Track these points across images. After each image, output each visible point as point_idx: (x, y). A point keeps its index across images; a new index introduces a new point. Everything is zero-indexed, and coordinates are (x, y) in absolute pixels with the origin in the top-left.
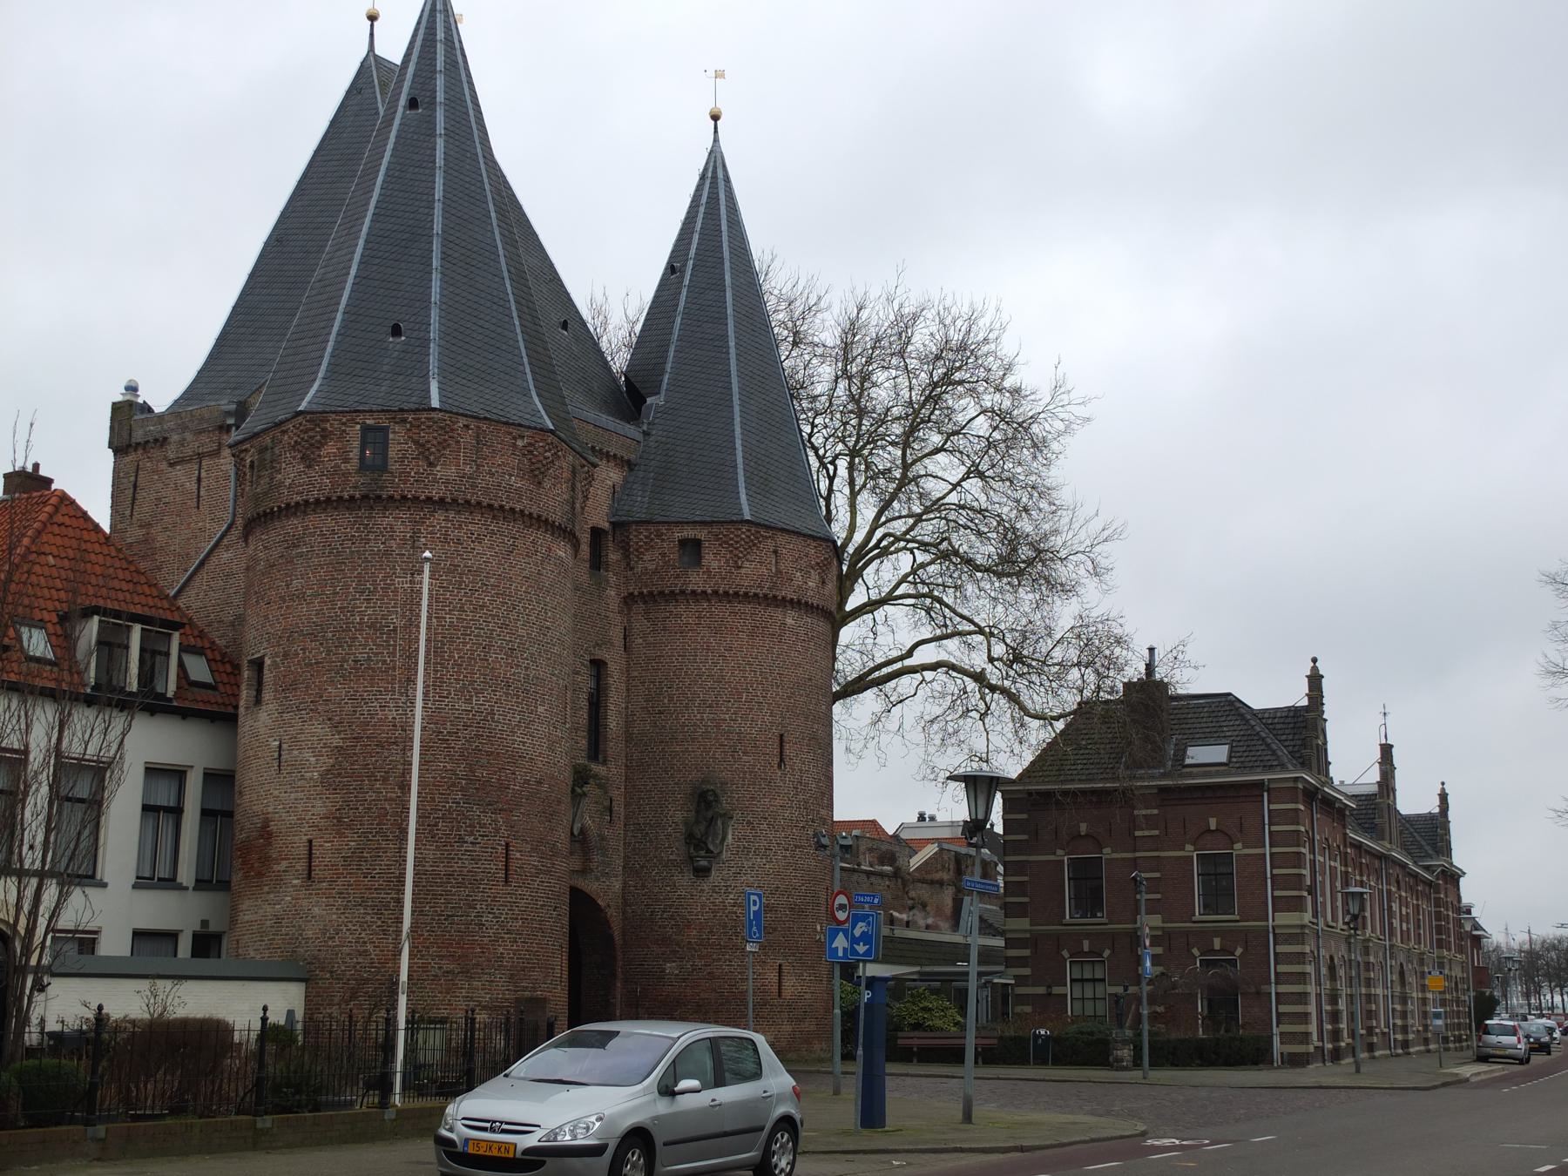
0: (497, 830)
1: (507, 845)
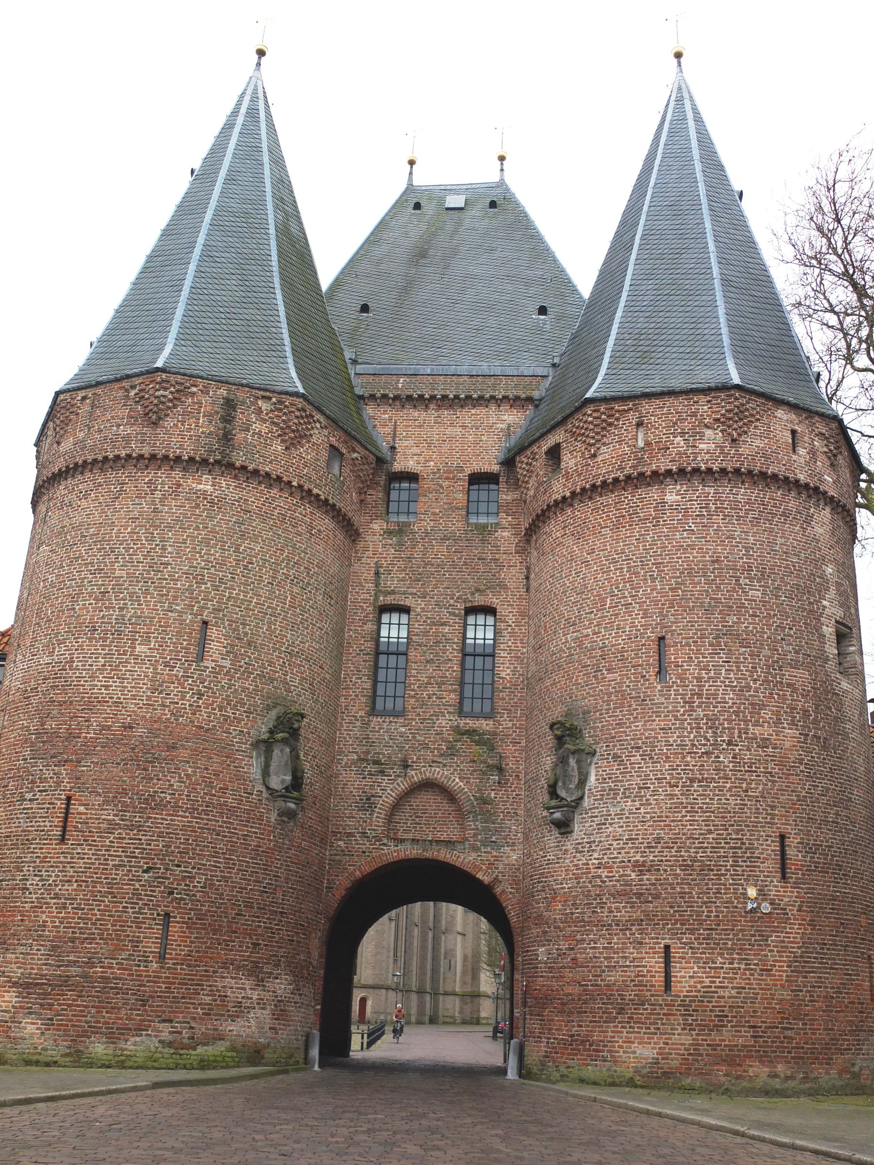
0: (58, 784)
1: (69, 799)
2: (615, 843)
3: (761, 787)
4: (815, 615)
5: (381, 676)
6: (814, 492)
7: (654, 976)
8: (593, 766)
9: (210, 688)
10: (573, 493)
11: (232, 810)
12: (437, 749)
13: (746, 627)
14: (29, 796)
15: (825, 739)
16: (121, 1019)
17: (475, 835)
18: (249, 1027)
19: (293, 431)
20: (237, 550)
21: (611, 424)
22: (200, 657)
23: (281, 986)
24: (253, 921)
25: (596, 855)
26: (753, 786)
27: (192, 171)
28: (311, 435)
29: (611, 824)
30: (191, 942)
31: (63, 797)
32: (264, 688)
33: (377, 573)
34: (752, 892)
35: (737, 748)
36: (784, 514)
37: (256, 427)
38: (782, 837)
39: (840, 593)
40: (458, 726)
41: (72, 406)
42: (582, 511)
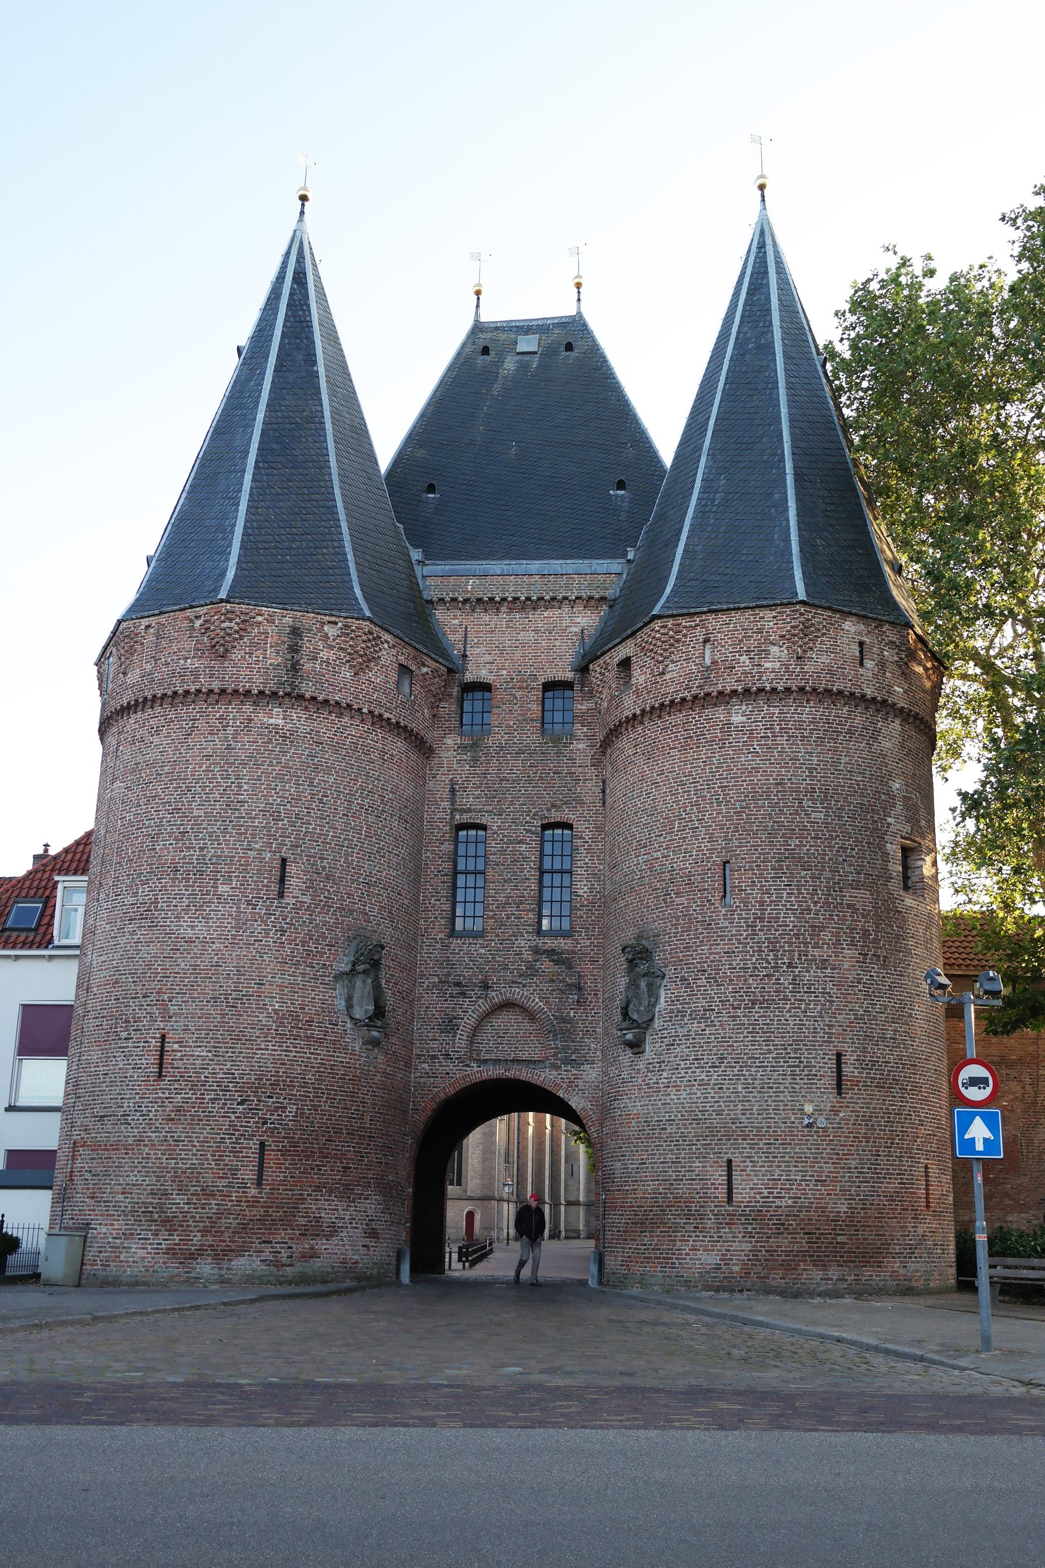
1: (163, 1037)
2: (682, 1063)
3: (819, 1007)
4: (878, 835)
5: (460, 897)
6: (882, 706)
7: (717, 1189)
8: (663, 988)
9: (292, 924)
10: (643, 711)
11: (320, 1041)
12: (517, 969)
13: (808, 850)
14: (124, 1035)
15: (885, 957)
16: (224, 1241)
17: (556, 1054)
18: (343, 1245)
19: (362, 656)
20: (311, 784)
21: (678, 641)
22: (281, 895)
23: (371, 1205)
24: (343, 1146)
25: (665, 1074)
26: (812, 1006)
27: (239, 350)
28: (379, 657)
29: (679, 1045)
30: (286, 1168)
31: (158, 1036)
32: (343, 921)
33: (453, 791)
34: (809, 1108)
35: (796, 970)
36: (849, 732)
37: (324, 654)
38: (839, 1055)
39: (907, 808)
40: (536, 946)
41: (137, 634)
42: (651, 729)
